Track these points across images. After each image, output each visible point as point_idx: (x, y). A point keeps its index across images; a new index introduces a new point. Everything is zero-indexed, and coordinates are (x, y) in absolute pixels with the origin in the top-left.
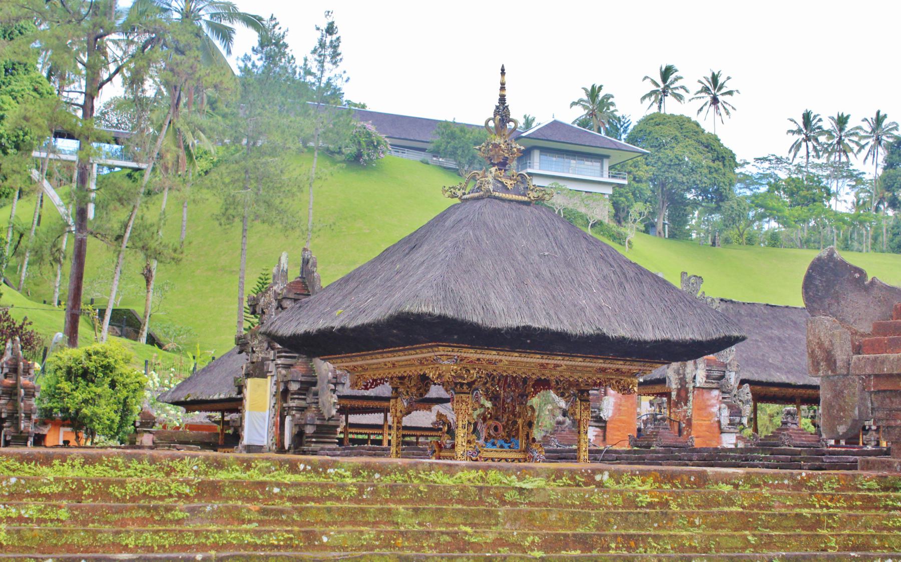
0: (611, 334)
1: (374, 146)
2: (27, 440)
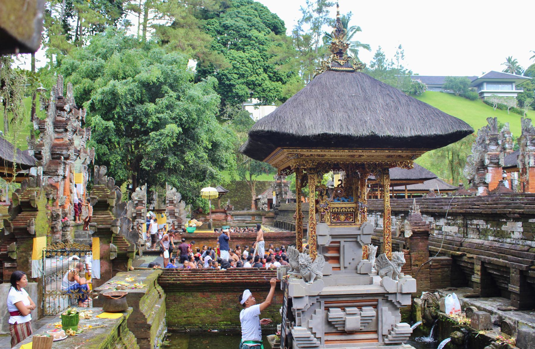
0: (381, 134)
1: (421, 87)
2: (286, 202)
